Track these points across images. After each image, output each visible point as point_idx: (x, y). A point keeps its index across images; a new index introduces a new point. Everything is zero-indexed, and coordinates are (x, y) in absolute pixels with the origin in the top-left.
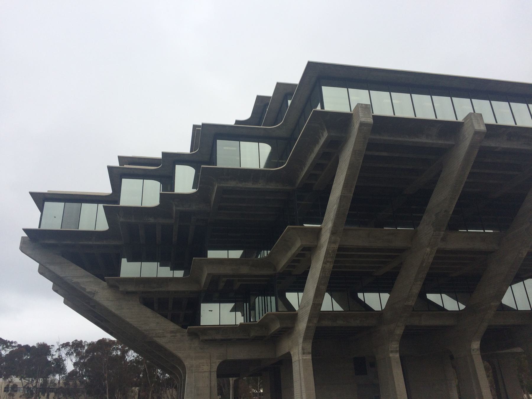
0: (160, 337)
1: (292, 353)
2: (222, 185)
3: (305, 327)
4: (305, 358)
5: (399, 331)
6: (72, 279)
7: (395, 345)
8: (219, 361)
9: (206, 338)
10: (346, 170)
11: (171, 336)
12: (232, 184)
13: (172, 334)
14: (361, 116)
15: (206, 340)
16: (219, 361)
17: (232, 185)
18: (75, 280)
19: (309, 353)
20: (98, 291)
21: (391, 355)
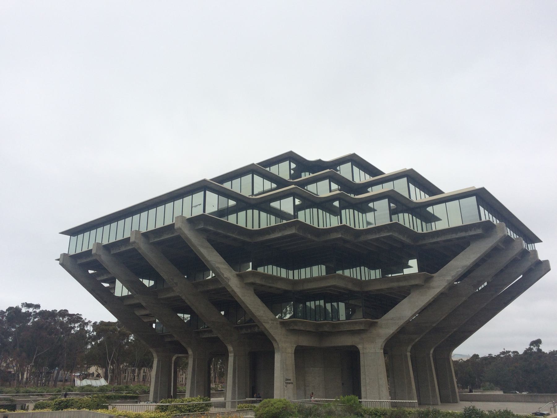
1: (360, 347)
5: (417, 340)
6: (216, 264)
7: (409, 348)
8: (295, 345)
9: (296, 328)
11: (272, 323)
12: (396, 235)
13: (272, 322)
15: (294, 330)
16: (295, 345)
18: (218, 265)
20: (231, 278)
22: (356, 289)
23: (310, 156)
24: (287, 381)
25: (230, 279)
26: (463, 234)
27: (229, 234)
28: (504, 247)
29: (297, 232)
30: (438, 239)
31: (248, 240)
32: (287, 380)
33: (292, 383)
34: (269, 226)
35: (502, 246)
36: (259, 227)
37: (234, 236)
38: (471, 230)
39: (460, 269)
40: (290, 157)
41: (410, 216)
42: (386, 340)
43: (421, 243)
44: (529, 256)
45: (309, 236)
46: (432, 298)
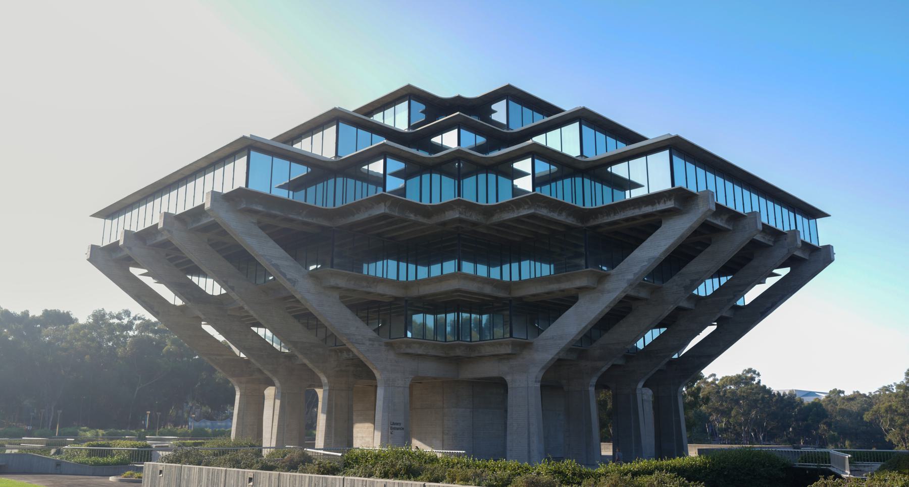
0: (359, 344)
1: (508, 379)
2: (537, 212)
3: (550, 358)
4: (536, 385)
5: (604, 369)
6: (272, 260)
8: (411, 376)
9: (409, 351)
10: (676, 238)
12: (544, 212)
13: (371, 342)
14: (710, 202)
15: (407, 354)
16: (411, 376)
17: (544, 214)
19: (539, 382)
21: (590, 389)
22: (501, 294)
23: (444, 91)
24: (393, 426)
25: (298, 281)
26: (648, 209)
27: (291, 216)
28: (730, 228)
29: (387, 211)
30: (616, 217)
31: (325, 223)
32: (394, 424)
33: (403, 429)
34: (344, 204)
35: (726, 226)
36: (334, 206)
37: (300, 218)
38: (659, 203)
39: (646, 263)
40: (409, 94)
41: (593, 182)
42: (543, 368)
43: (593, 223)
44: (786, 240)
45: (412, 217)
46: (606, 307)
